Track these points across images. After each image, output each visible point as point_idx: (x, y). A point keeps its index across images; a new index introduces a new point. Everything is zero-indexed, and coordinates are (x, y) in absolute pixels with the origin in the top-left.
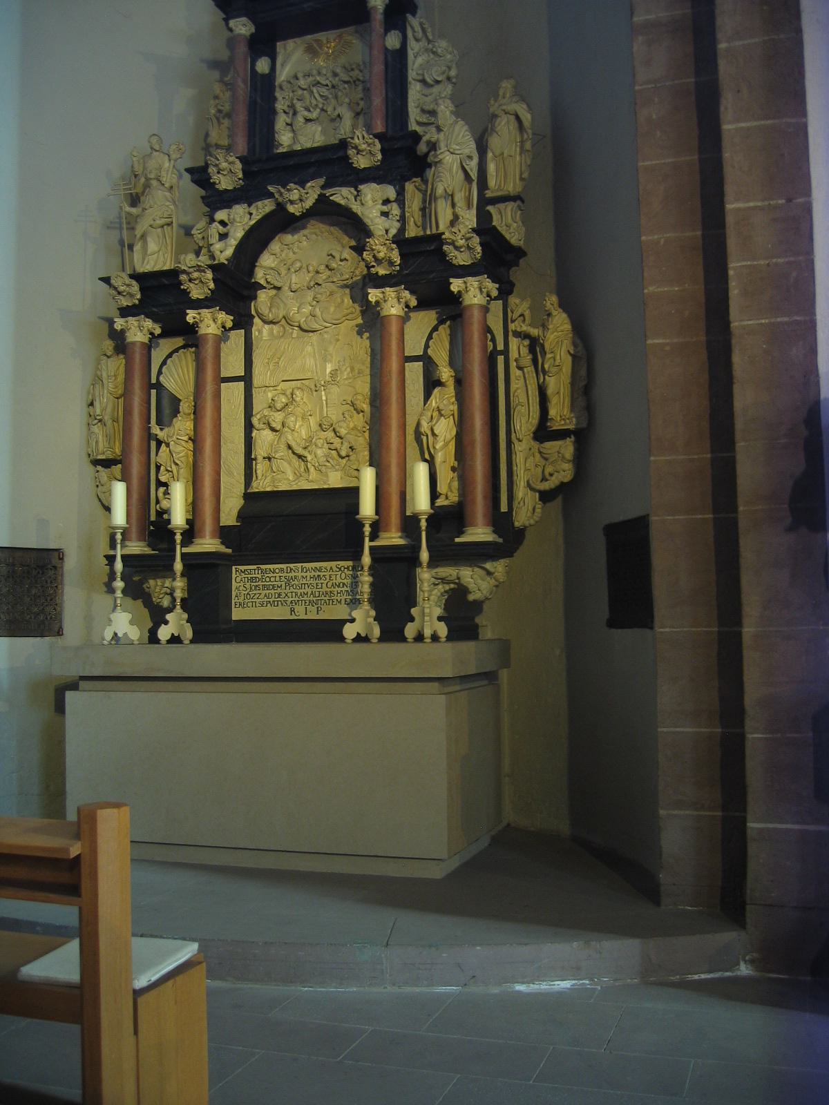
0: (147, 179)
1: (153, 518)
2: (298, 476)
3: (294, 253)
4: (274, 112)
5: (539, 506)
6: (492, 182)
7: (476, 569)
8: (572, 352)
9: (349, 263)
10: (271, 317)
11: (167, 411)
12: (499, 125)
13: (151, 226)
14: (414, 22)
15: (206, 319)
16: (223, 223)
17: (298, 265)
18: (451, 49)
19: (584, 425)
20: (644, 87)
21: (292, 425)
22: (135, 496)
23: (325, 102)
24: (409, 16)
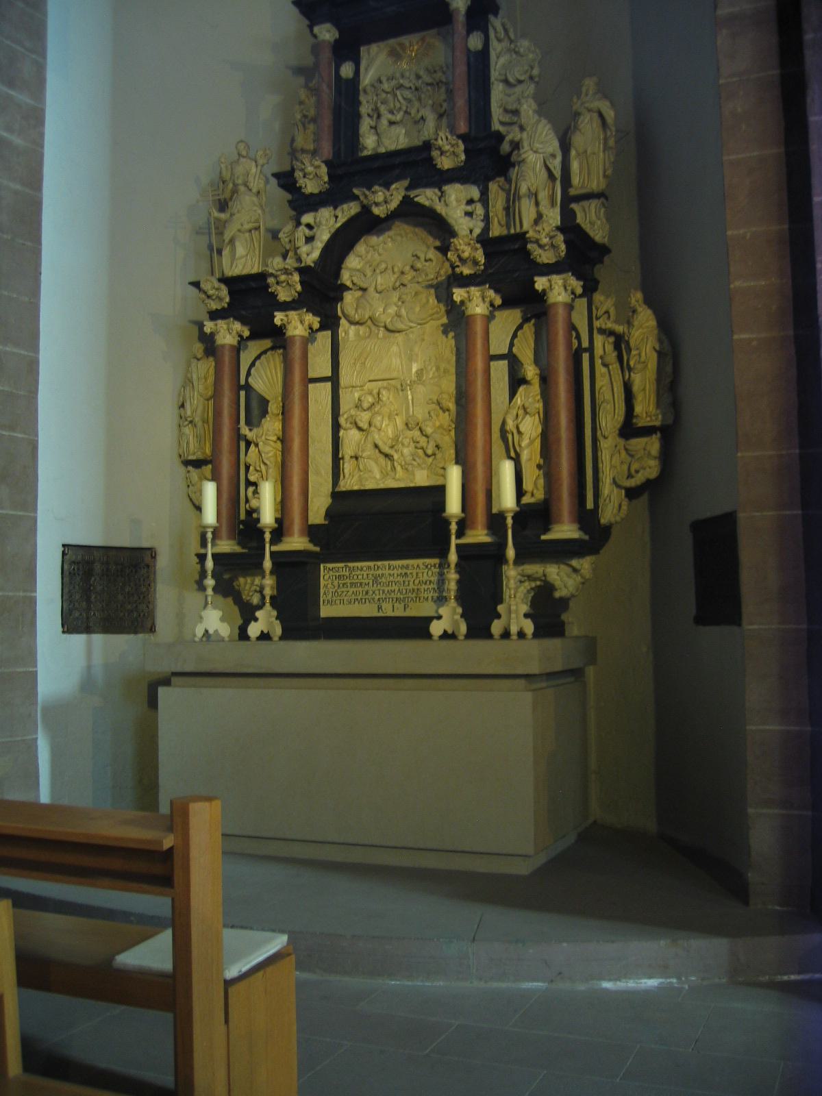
0: (235, 185)
1: (243, 516)
2: (385, 475)
3: (380, 255)
4: (358, 116)
5: (625, 503)
6: (576, 180)
7: (562, 566)
9: (434, 263)
11: (256, 411)
12: (581, 123)
13: (239, 231)
14: (496, 22)
15: (293, 322)
16: (309, 226)
17: (383, 266)
18: (533, 48)
19: (670, 421)
21: (378, 424)
22: (225, 496)
23: (409, 105)
24: (492, 18)
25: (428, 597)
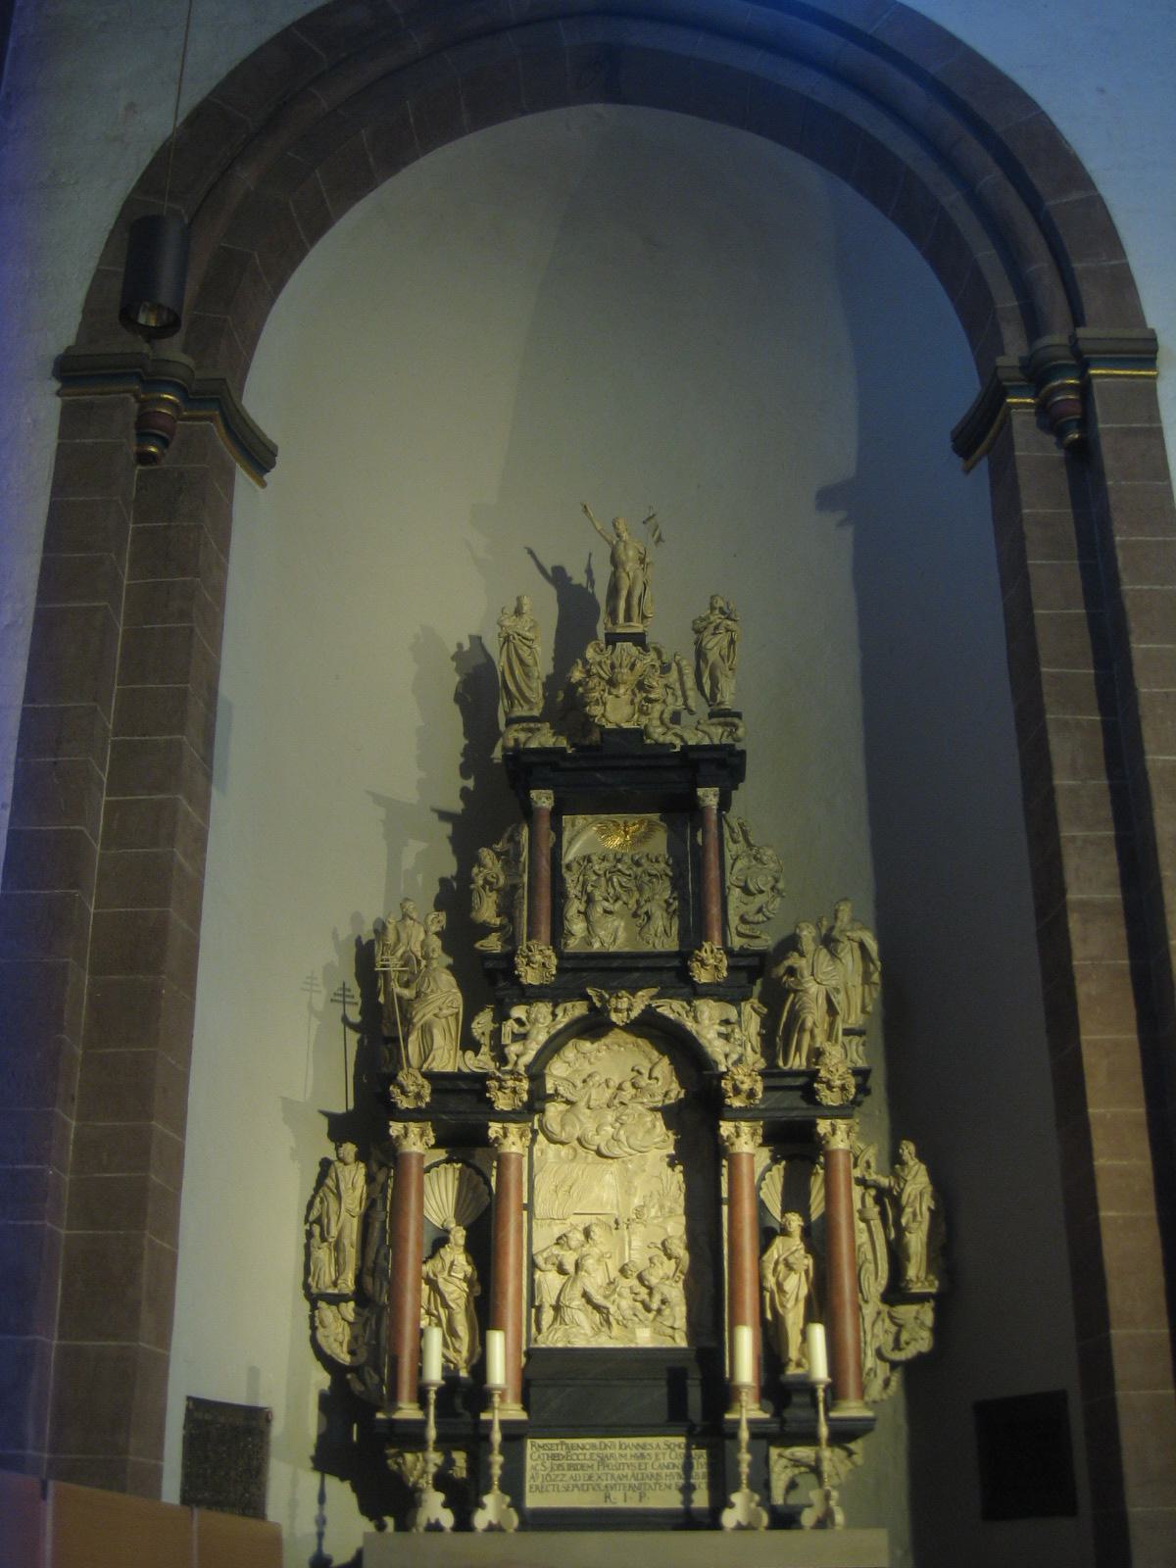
2: (597, 1332)
3: (591, 1063)
8: (933, 1207)
9: (660, 1083)
10: (563, 1136)
12: (842, 951)
16: (519, 1021)
20: (1082, 962)
25: (671, 1485)
